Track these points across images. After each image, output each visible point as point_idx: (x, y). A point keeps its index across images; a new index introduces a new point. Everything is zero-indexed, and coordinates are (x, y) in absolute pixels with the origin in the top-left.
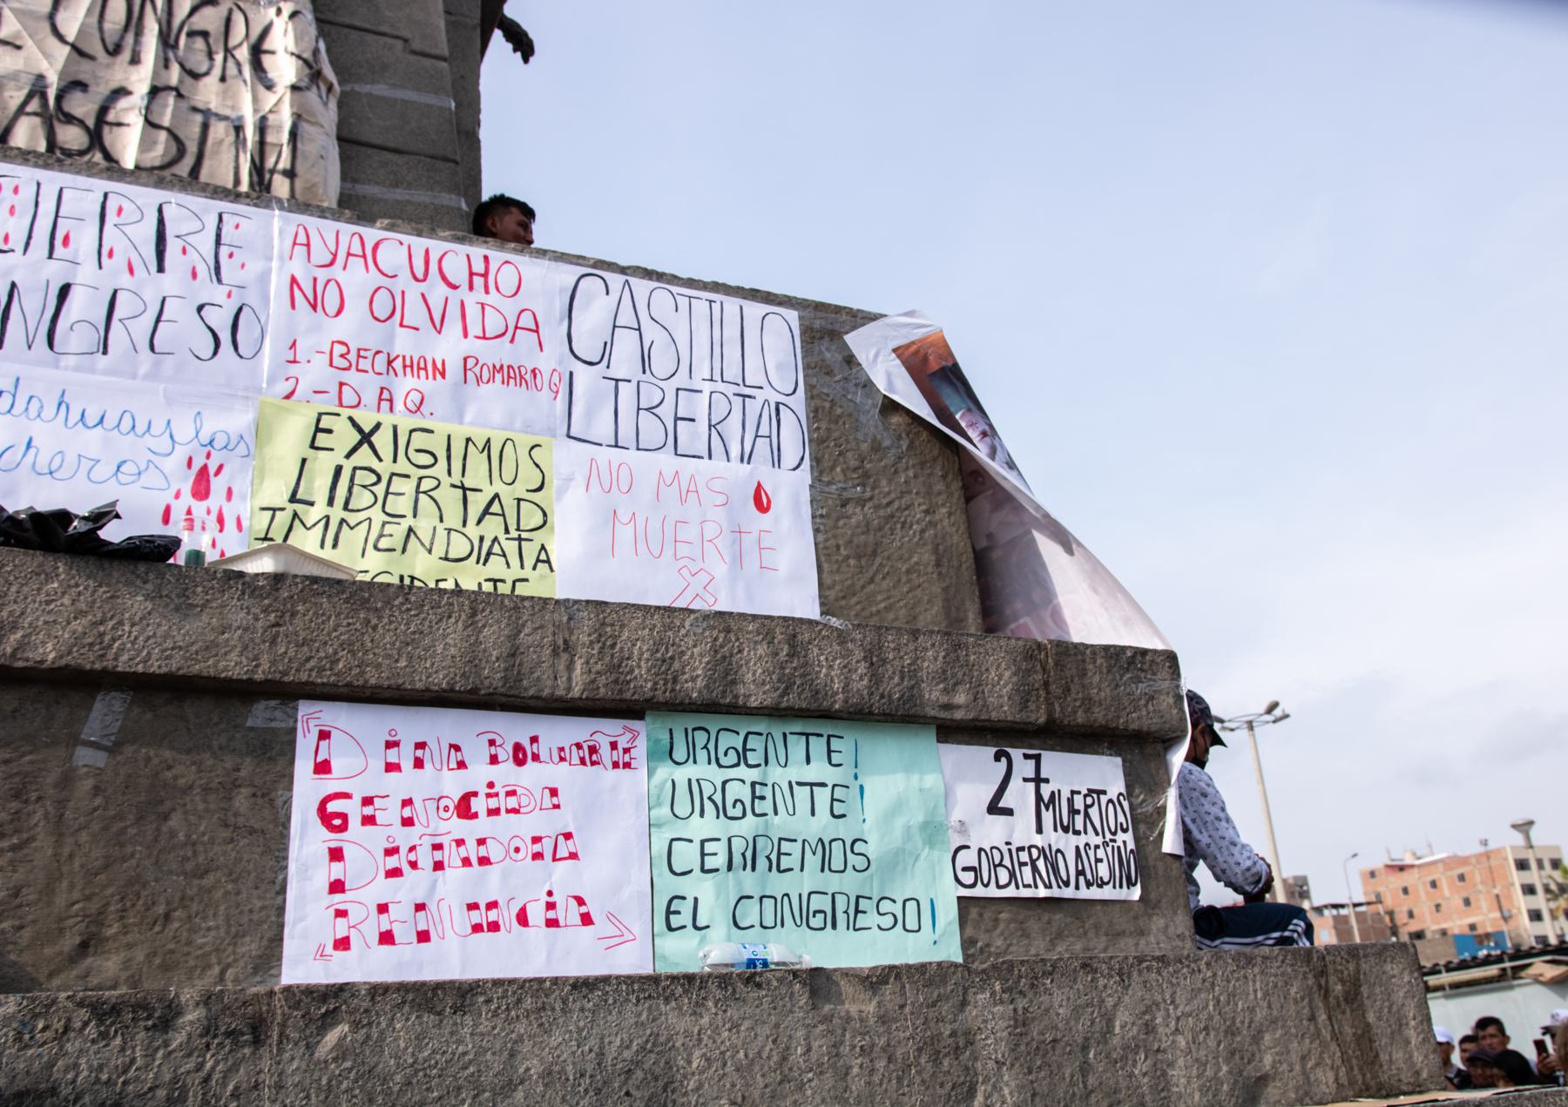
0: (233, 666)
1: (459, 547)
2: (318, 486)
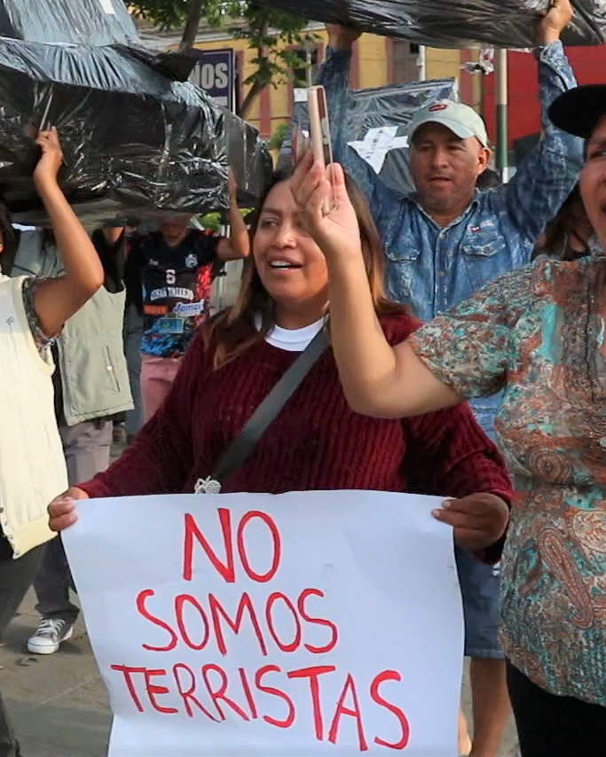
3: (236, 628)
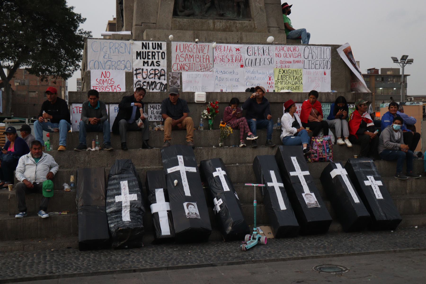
0: (279, 101)
1: (293, 83)
2: (280, 78)
3: (105, 82)
